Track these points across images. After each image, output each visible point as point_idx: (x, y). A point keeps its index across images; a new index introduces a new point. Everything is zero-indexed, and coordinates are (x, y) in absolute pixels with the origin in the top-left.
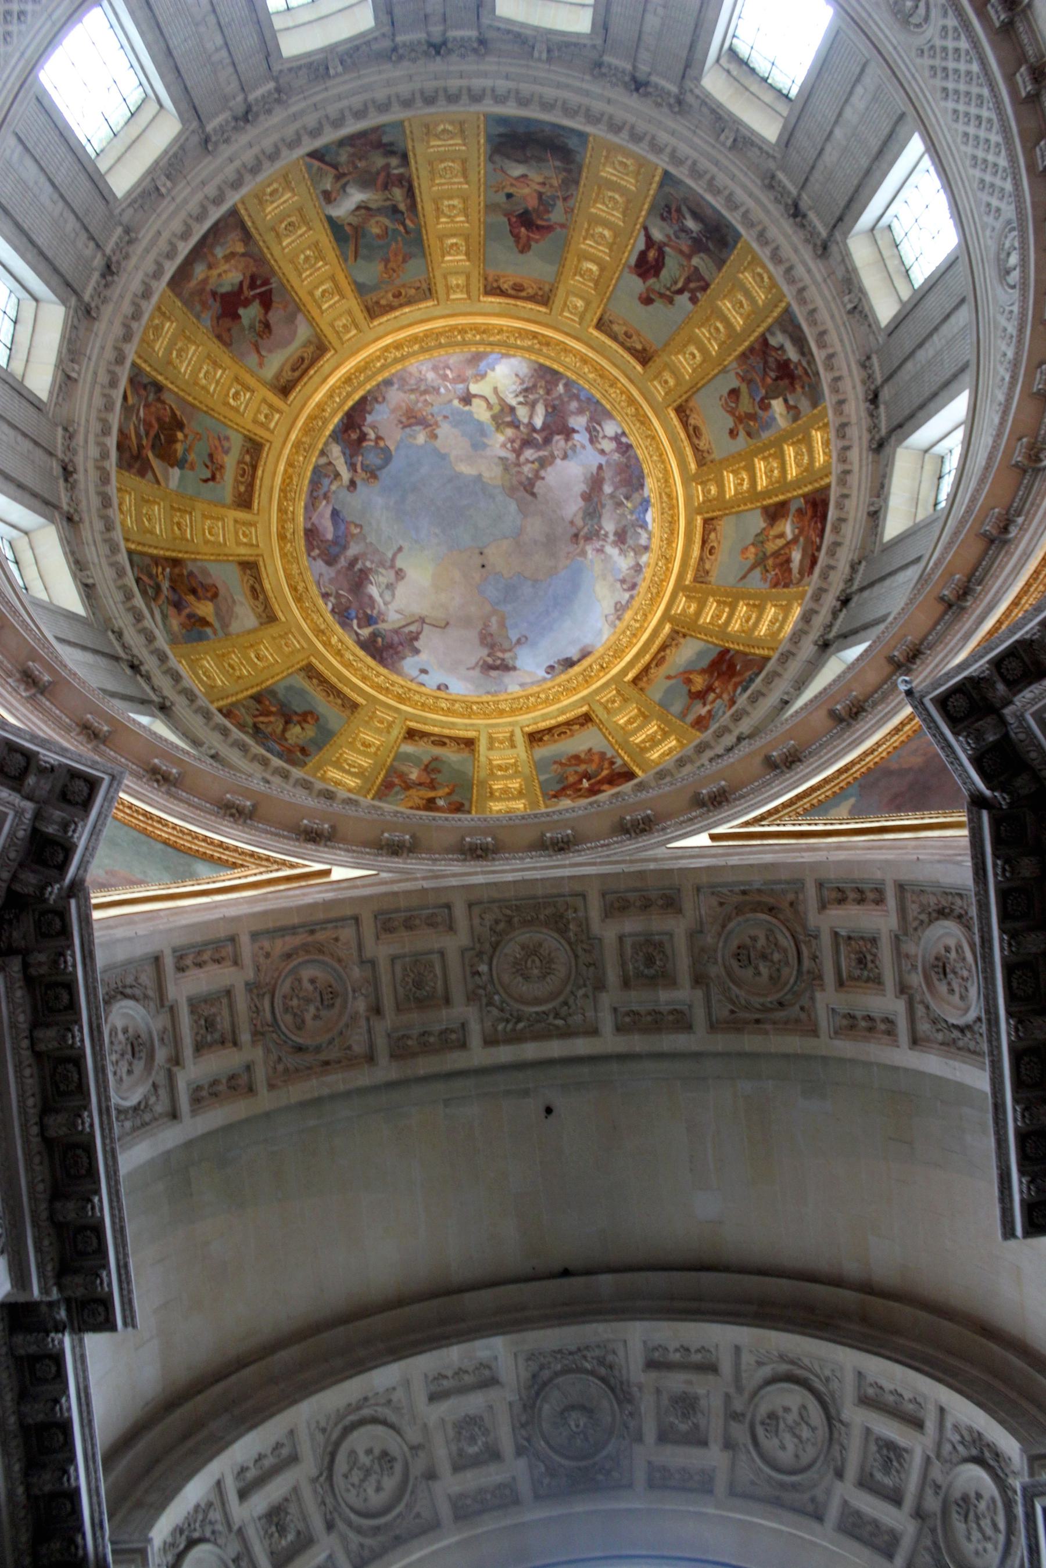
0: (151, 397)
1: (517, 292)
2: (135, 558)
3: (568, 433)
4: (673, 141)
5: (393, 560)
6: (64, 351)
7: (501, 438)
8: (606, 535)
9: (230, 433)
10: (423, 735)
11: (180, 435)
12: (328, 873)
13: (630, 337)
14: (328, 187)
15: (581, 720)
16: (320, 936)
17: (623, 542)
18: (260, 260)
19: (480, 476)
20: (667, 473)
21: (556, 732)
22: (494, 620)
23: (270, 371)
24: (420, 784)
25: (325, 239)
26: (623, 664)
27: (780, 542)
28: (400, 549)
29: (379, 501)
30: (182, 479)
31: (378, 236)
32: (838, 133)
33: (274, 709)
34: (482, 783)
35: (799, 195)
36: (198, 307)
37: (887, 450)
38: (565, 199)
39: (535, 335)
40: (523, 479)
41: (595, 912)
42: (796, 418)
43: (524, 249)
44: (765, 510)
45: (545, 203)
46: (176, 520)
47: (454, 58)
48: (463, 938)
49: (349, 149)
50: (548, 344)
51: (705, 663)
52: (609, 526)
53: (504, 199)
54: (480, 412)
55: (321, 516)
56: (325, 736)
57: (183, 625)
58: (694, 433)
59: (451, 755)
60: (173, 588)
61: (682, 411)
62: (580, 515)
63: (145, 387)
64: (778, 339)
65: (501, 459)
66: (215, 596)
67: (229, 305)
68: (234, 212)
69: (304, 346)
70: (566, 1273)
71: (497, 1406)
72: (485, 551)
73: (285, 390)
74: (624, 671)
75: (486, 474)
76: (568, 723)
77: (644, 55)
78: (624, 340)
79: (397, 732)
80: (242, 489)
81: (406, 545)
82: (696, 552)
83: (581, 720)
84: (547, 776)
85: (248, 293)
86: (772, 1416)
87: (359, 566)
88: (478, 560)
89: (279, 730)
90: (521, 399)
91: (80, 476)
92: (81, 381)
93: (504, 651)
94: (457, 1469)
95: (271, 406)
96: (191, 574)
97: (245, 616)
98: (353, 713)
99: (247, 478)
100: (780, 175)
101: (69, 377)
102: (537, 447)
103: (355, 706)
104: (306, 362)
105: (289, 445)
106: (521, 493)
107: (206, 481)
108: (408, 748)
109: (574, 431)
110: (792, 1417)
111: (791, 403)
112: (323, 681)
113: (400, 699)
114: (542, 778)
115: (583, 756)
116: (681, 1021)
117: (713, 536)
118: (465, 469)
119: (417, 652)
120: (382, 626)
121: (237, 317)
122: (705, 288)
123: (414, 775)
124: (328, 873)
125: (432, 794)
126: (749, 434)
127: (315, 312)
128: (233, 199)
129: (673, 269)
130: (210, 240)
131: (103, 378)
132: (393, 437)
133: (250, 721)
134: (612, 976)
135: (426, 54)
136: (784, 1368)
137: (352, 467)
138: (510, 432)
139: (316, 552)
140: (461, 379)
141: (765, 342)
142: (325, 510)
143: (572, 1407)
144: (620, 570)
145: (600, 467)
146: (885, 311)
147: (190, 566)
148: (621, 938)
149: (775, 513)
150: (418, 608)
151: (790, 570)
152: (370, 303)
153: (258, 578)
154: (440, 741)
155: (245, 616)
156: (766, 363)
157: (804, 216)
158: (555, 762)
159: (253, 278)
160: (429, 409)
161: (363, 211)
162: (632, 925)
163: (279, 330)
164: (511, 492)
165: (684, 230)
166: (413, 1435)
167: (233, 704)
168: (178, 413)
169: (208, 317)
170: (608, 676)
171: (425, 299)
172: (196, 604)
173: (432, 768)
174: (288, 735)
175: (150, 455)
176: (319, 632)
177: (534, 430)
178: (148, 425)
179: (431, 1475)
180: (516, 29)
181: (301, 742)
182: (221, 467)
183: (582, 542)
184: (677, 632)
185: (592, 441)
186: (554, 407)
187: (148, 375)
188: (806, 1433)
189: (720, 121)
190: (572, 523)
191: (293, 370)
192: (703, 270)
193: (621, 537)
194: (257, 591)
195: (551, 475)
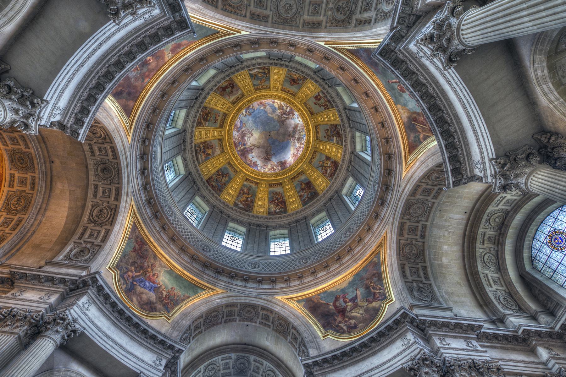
1: (288, 92)
3: (293, 115)
10: (250, 180)
18: (233, 81)
23: (231, 100)
25: (248, 77)
29: (251, 119)
42: (338, 143)
43: (292, 85)
44: (326, 156)
51: (305, 182)
52: (297, 136)
56: (230, 179)
58: (317, 133)
59: (253, 186)
61: (316, 127)
67: (224, 89)
70: (245, 344)
72: (272, 133)
76: (277, 184)
79: (244, 179)
88: (269, 134)
94: (223, 370)
102: (286, 115)
103: (237, 172)
108: (245, 183)
112: (232, 166)
113: (246, 170)
118: (270, 115)
122: (328, 109)
137: (246, 112)
142: (239, 120)
153: (222, 143)
155: (218, 151)
163: (234, 92)
164: (279, 122)
166: (218, 365)
169: (219, 92)
179: (219, 370)
193: (299, 139)
195: (288, 121)
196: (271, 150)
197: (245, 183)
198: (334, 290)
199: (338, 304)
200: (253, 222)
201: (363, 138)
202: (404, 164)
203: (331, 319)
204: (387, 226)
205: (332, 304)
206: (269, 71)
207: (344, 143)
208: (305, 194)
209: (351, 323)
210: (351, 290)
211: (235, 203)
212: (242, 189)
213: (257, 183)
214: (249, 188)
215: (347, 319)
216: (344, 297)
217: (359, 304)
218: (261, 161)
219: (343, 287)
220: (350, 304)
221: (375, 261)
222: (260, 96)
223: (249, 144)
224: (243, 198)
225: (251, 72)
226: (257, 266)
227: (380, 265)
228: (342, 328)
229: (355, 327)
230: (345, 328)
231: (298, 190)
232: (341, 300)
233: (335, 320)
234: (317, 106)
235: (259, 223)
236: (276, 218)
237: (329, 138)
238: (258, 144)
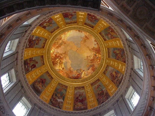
0: (99, 100)
1: (50, 75)
2: (117, 85)
3: (56, 55)
4: (23, 77)
5: (86, 59)
6: (106, 113)
7: (63, 61)
9: (93, 88)
10: (104, 39)
11: (99, 93)
12: (151, 43)
13: (42, 60)
14: (61, 104)
17: (61, 38)
18: (74, 103)
19: (69, 59)
20: (51, 42)
21: (90, 26)
22: (82, 43)
23: (83, 91)
24: (110, 34)
25: (65, 99)
26: (75, 26)
27: (47, 24)
28: (85, 59)
30: (103, 88)
31: (60, 94)
32: (8, 65)
33: (117, 57)
35: (15, 61)
36: (86, 104)
37: (30, 24)
38: (37, 81)
39: (51, 69)
40: (65, 55)
41: (131, 12)
42: (33, 36)
43: (45, 79)
44: (45, 29)
45: (39, 82)
46: (108, 85)
47: (39, 106)
49: (56, 106)
50: (51, 67)
51: (67, 18)
52: (61, 41)
53: (43, 86)
55: (90, 71)
56: (115, 49)
57: (118, 74)
58: (44, 44)
59: (103, 34)
60: (115, 79)
61: (44, 47)
62: (62, 45)
63: (99, 101)
65: (65, 59)
66: (111, 74)
67: (82, 101)
68: (74, 110)
69: (77, 90)
73: (83, 87)
74: (76, 25)
75: (68, 59)
76: (87, 25)
77: (20, 90)
78: (43, 60)
80: (97, 81)
84: (96, 22)
87: (91, 62)
88: (77, 50)
90: (58, 63)
91: (116, 99)
92: (107, 108)
95: (86, 87)
96: (112, 78)
98: (109, 48)
100: (15, 64)
101: (108, 110)
102: (60, 56)
103: (108, 49)
104: (78, 88)
105: (88, 81)
106: (66, 53)
107: (101, 86)
108: (107, 39)
109: (55, 55)
111: (32, 38)
112: (109, 54)
115: (90, 21)
118: (70, 61)
119: (94, 47)
120: (95, 53)
121: (82, 99)
122: (30, 58)
123: (110, 36)
124: (151, 43)
125: (110, 32)
126: (39, 38)
127: (73, 92)
128: (74, 112)
129: (32, 64)
130: (79, 109)
131: (104, 106)
132: (75, 72)
133: (121, 58)
135: (42, 108)
137: (82, 73)
138: (62, 61)
139: (94, 67)
140: (62, 71)
141: (29, 47)
144: (64, 35)
145: (56, 48)
146: (17, 41)
148: (131, 7)
150: (88, 51)
151: (49, 20)
153: (105, 71)
154: (103, 36)
155: (110, 69)
157: (16, 58)
158: (94, 23)
159: (77, 101)
160: (68, 71)
161: (59, 98)
162: (128, 7)
167: (122, 62)
168: (97, 95)
169: (85, 102)
170: (78, 26)
171: (60, 83)
172: (114, 75)
173: (107, 35)
174: (119, 53)
175: (105, 94)
176: (104, 60)
177: (59, 59)
178: (102, 97)
180: (30, 103)
181: (118, 51)
182: (97, 86)
183: (65, 42)
184: (66, 24)
187: (97, 102)
189: (17, 76)
192: (29, 61)
193: (61, 39)
194: (106, 70)
195: (62, 52)
196: (82, 41)
204: (1, 27)
206: (53, 96)
213: (100, 33)
222: (67, 81)
225: (62, 101)
237: (38, 39)
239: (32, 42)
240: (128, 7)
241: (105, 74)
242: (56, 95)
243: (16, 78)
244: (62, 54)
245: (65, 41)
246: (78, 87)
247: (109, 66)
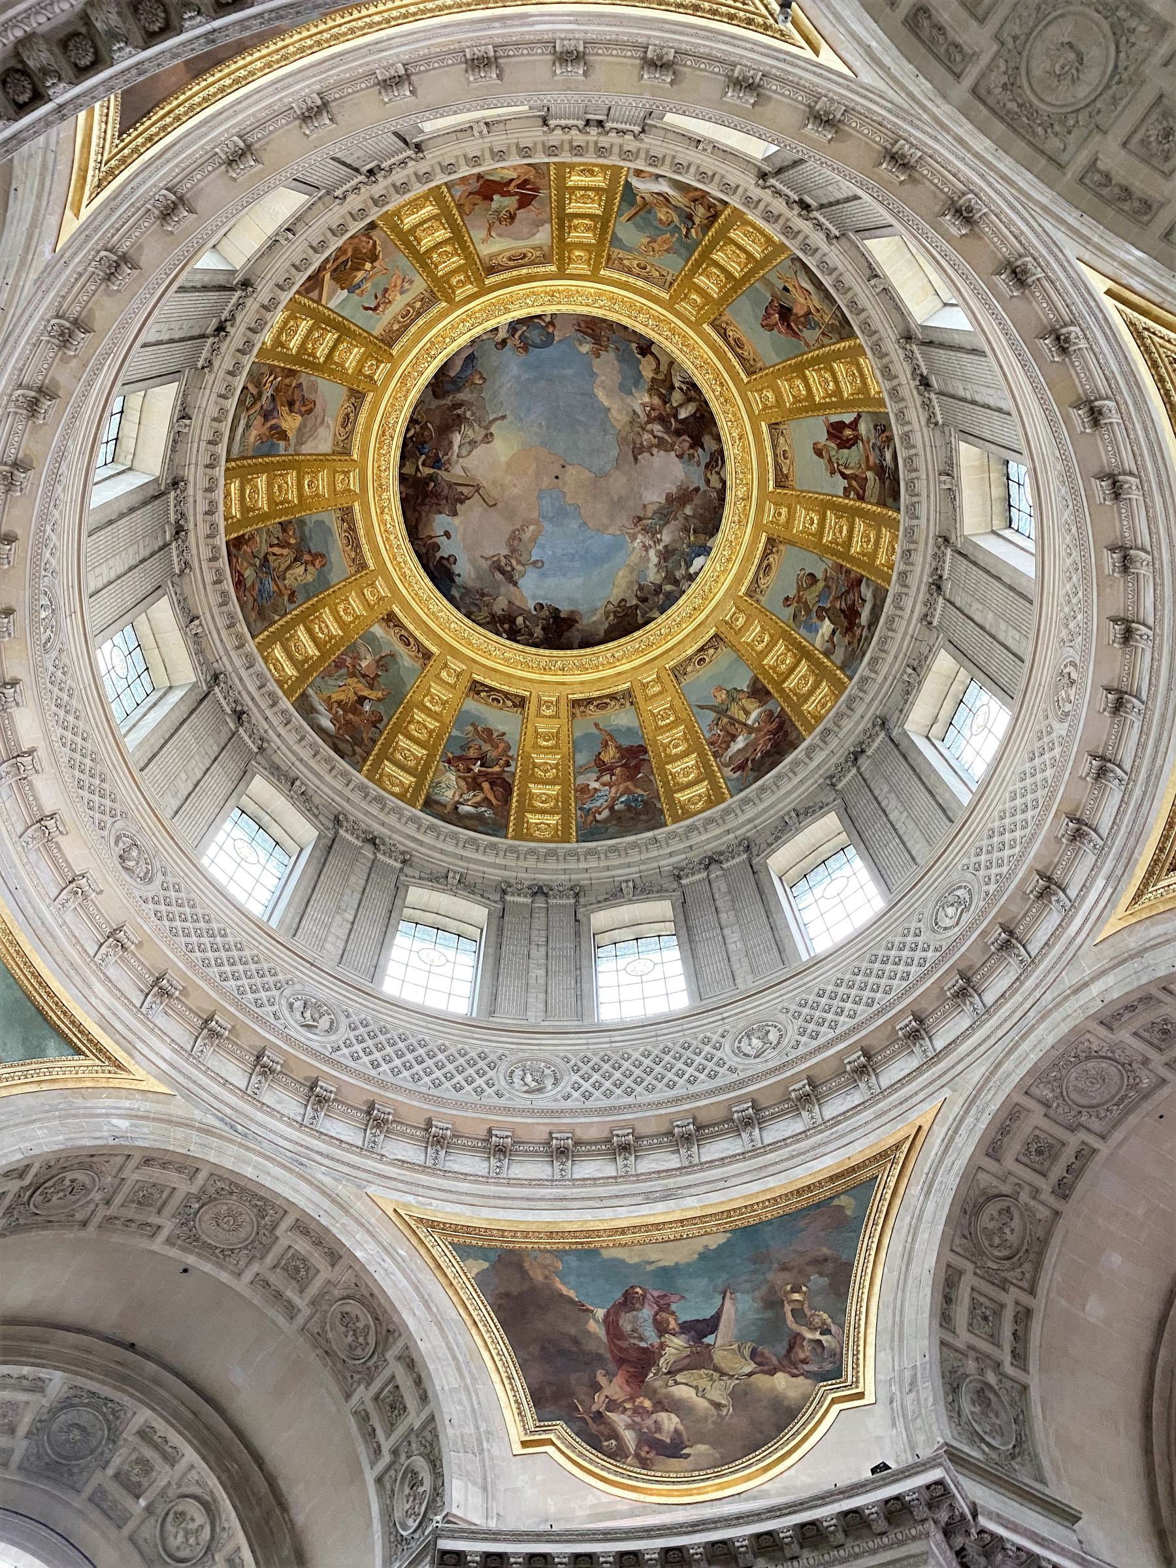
1: (736, 345)
3: (697, 443)
5: (491, 422)
7: (646, 399)
8: (660, 541)
10: (400, 625)
11: (368, 266)
15: (517, 701)
16: (95, 1159)
17: (666, 560)
27: (742, 717)
28: (504, 417)
29: (515, 370)
33: (293, 541)
34: (408, 709)
42: (827, 653)
48: (194, 1189)
51: (625, 743)
52: (666, 537)
54: (647, 368)
58: (765, 568)
59: (407, 658)
62: (656, 507)
64: (867, 592)
65: (634, 412)
66: (310, 411)
71: (31, 1408)
73: (491, 270)
75: (614, 413)
76: (506, 695)
80: (396, 327)
81: (510, 418)
82: (690, 652)
83: (517, 701)
85: (511, 188)
86: (182, 1514)
88: (556, 469)
89: (283, 567)
93: (519, 562)
97: (323, 442)
99: (407, 320)
102: (667, 430)
103: (364, 566)
107: (366, 309)
108: (378, 630)
110: (193, 1526)
112: (352, 529)
114: (455, 733)
116: (291, 1311)
117: (711, 651)
118: (601, 395)
122: (861, 498)
125: (366, 693)
126: (795, 617)
129: (852, 457)
133: (265, 548)
134: (270, 1259)
136: (207, 1498)
138: (656, 401)
141: (859, 582)
143: (78, 1426)
145: (697, 490)
147: (303, 380)
149: (759, 692)
152: (614, 256)
153: (357, 409)
156: (847, 592)
158: (473, 724)
159: (526, 181)
160: (609, 333)
162: (302, 1246)
165: (882, 455)
177: (675, 416)
185: (707, 466)
186: (702, 416)
188: (192, 1541)
190: (645, 506)
191: (510, 259)
192: (870, 484)
193: (667, 554)
194: (348, 421)
196: (534, 539)
197: (378, 630)
198: (631, 1257)
199: (626, 1323)
200: (355, 814)
201: (957, 687)
202: (1132, 891)
203: (575, 1379)
204: (947, 1092)
205: (600, 1313)
206: (715, 217)
207: (863, 669)
208: (607, 793)
209: (658, 1427)
210: (702, 1283)
211: (304, 695)
212: (353, 651)
213: (428, 655)
214: (386, 662)
215: (647, 1404)
216: (663, 1307)
217: (718, 1357)
218: (473, 561)
219: (669, 1257)
220: (676, 1345)
221: (841, 1208)
222: (613, 299)
223: (457, 470)
224: (346, 690)
225: (635, 182)
226: (324, 1023)
227: (857, 1230)
228: (616, 1436)
229: (674, 1449)
230: (629, 1438)
231: (583, 758)
232: (647, 1313)
233: (597, 1388)
234: (822, 463)
235: (378, 829)
236: (454, 836)
238: (494, 493)
239: (842, 611)
240: (302, 1246)
241: (351, 390)
242: (690, 217)
243: (958, 459)
244: (653, 446)
245: (640, 537)
246: (532, 263)
247: (333, 453)
